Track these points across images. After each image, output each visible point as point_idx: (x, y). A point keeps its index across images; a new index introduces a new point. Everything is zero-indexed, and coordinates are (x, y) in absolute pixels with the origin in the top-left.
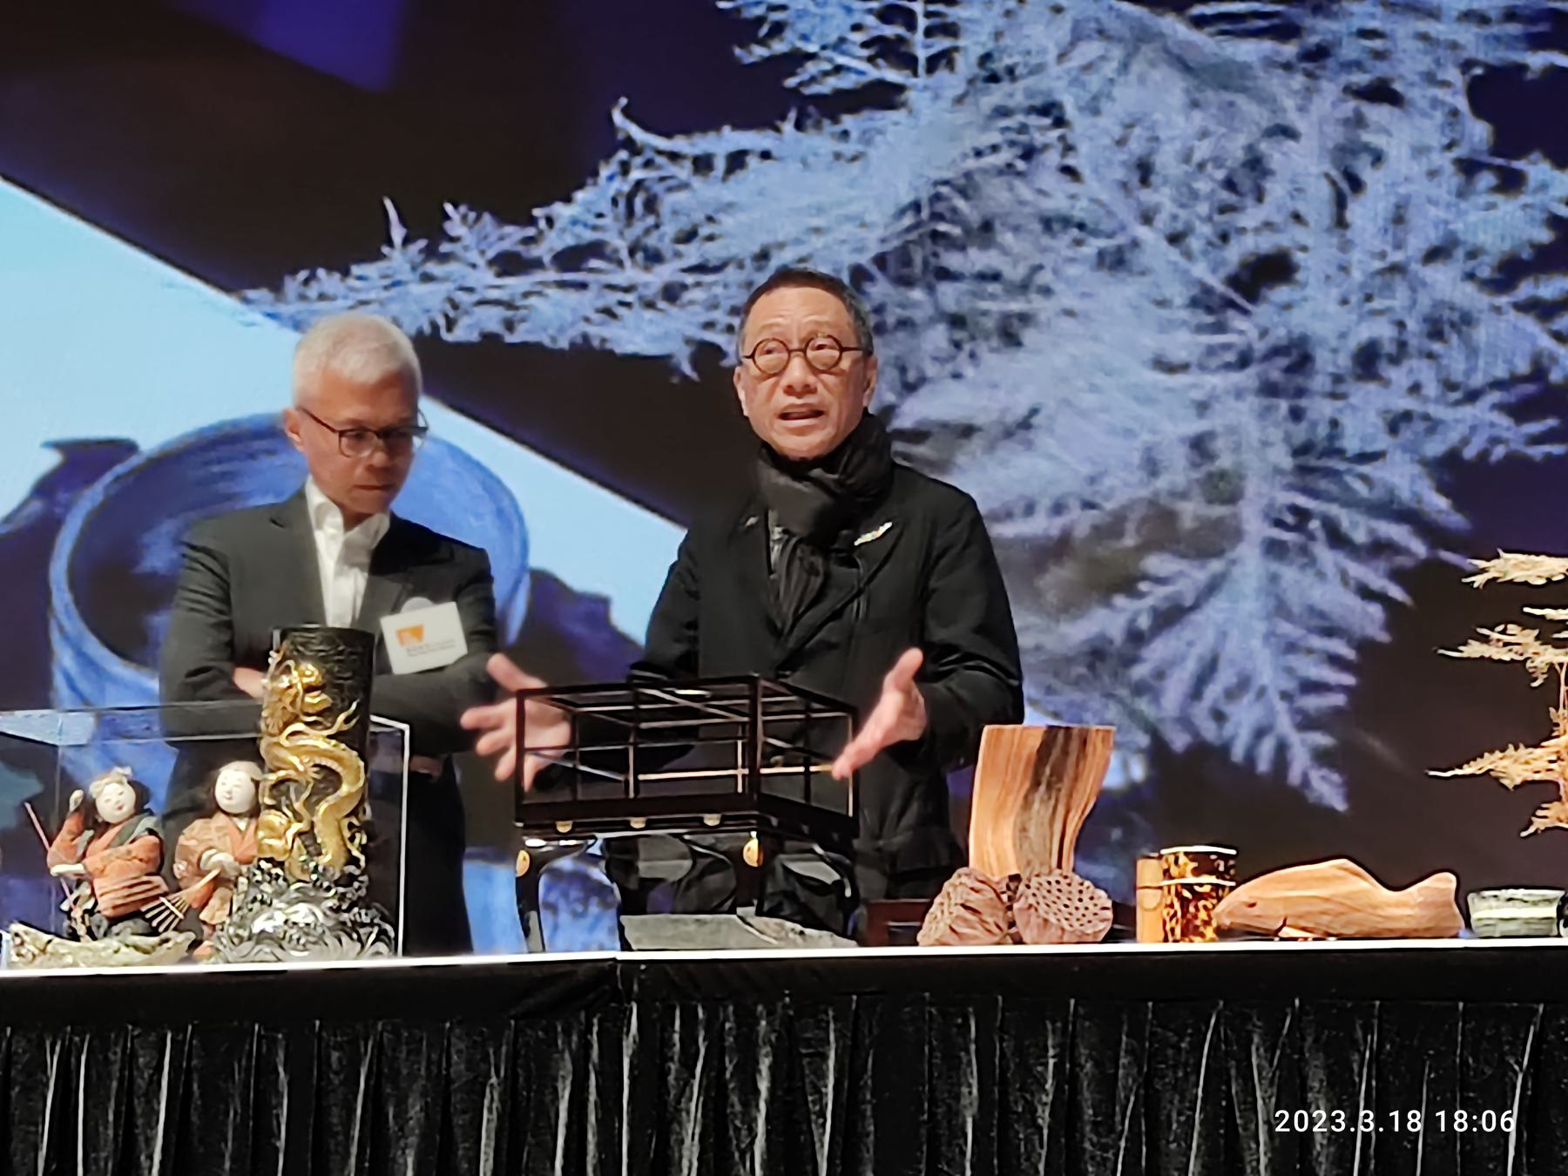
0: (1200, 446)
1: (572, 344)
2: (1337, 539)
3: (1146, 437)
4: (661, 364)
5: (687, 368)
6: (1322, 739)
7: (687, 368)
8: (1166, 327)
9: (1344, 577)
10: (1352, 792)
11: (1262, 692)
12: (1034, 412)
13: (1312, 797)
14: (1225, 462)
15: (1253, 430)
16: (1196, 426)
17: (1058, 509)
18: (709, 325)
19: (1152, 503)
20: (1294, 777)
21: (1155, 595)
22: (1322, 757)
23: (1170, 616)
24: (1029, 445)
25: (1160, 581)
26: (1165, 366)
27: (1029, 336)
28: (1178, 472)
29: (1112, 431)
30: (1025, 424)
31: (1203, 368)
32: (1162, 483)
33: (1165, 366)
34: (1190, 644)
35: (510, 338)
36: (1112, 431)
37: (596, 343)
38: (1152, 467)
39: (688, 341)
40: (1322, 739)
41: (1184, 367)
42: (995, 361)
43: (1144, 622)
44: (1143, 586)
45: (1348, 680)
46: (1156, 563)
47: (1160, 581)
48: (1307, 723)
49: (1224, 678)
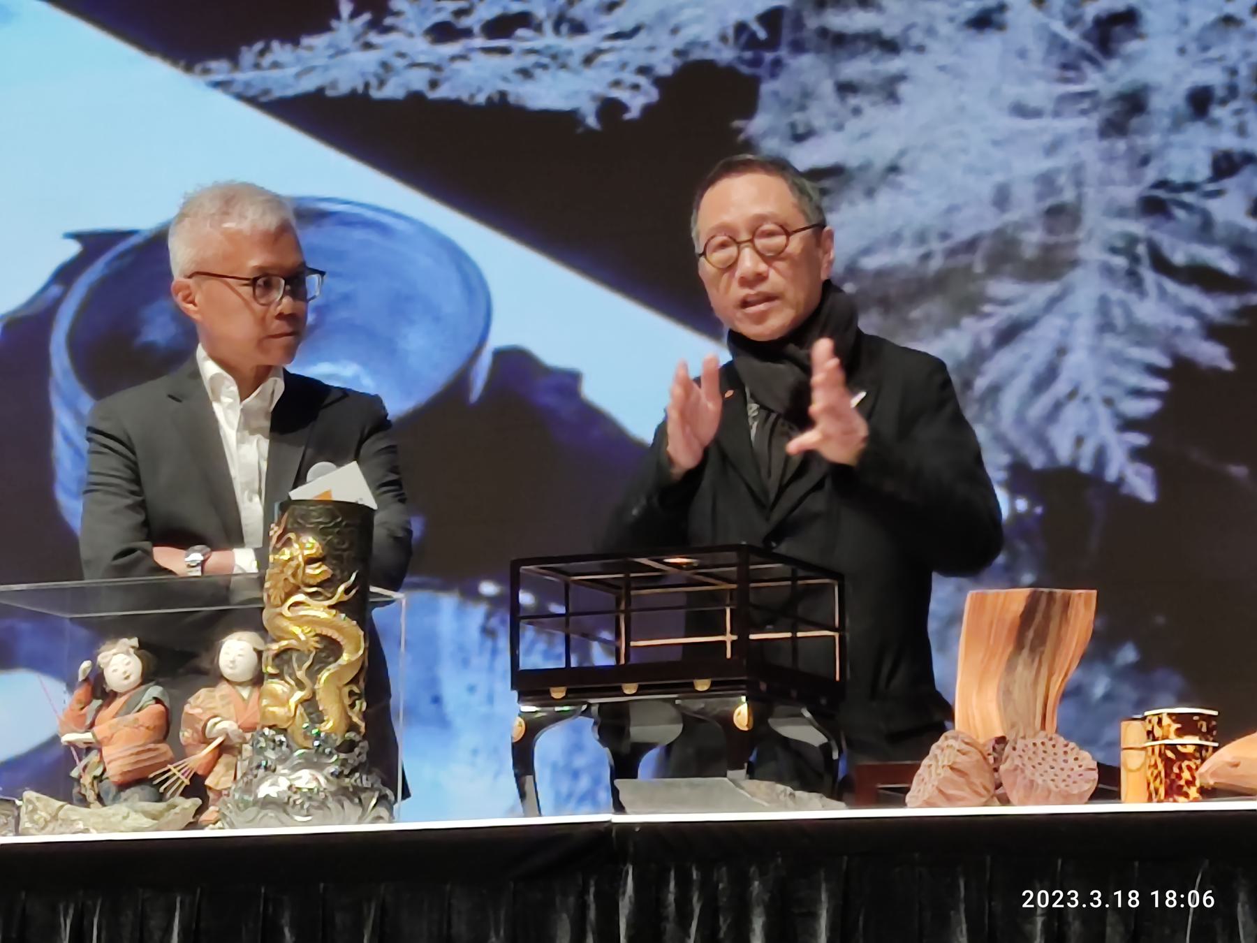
0: (1047, 182)
1: (489, 99)
2: (1162, 265)
3: (999, 178)
4: (569, 118)
5: (592, 121)
6: (1139, 439)
7: (592, 121)
8: (1024, 79)
9: (1163, 293)
10: (1163, 482)
11: (1086, 399)
12: (902, 153)
13: (1125, 490)
14: (1068, 196)
15: (1095, 168)
16: (1046, 164)
17: (921, 238)
18: (617, 84)
19: (999, 233)
20: (1111, 474)
21: (999, 317)
22: (1138, 454)
23: (1009, 334)
24: (898, 187)
25: (1005, 303)
26: (1021, 110)
27: (904, 89)
28: (1026, 206)
29: (970, 169)
30: (894, 169)
31: (1057, 114)
32: (1012, 216)
33: (1021, 110)
34: (1027, 358)
35: (434, 95)
36: (970, 169)
37: (512, 99)
38: (1002, 199)
39: (594, 98)
40: (1139, 439)
41: (1036, 113)
42: (875, 113)
43: (987, 340)
44: (987, 308)
45: (1160, 385)
46: (1002, 288)
47: (1005, 303)
48: (1128, 424)
49: (1061, 387)
